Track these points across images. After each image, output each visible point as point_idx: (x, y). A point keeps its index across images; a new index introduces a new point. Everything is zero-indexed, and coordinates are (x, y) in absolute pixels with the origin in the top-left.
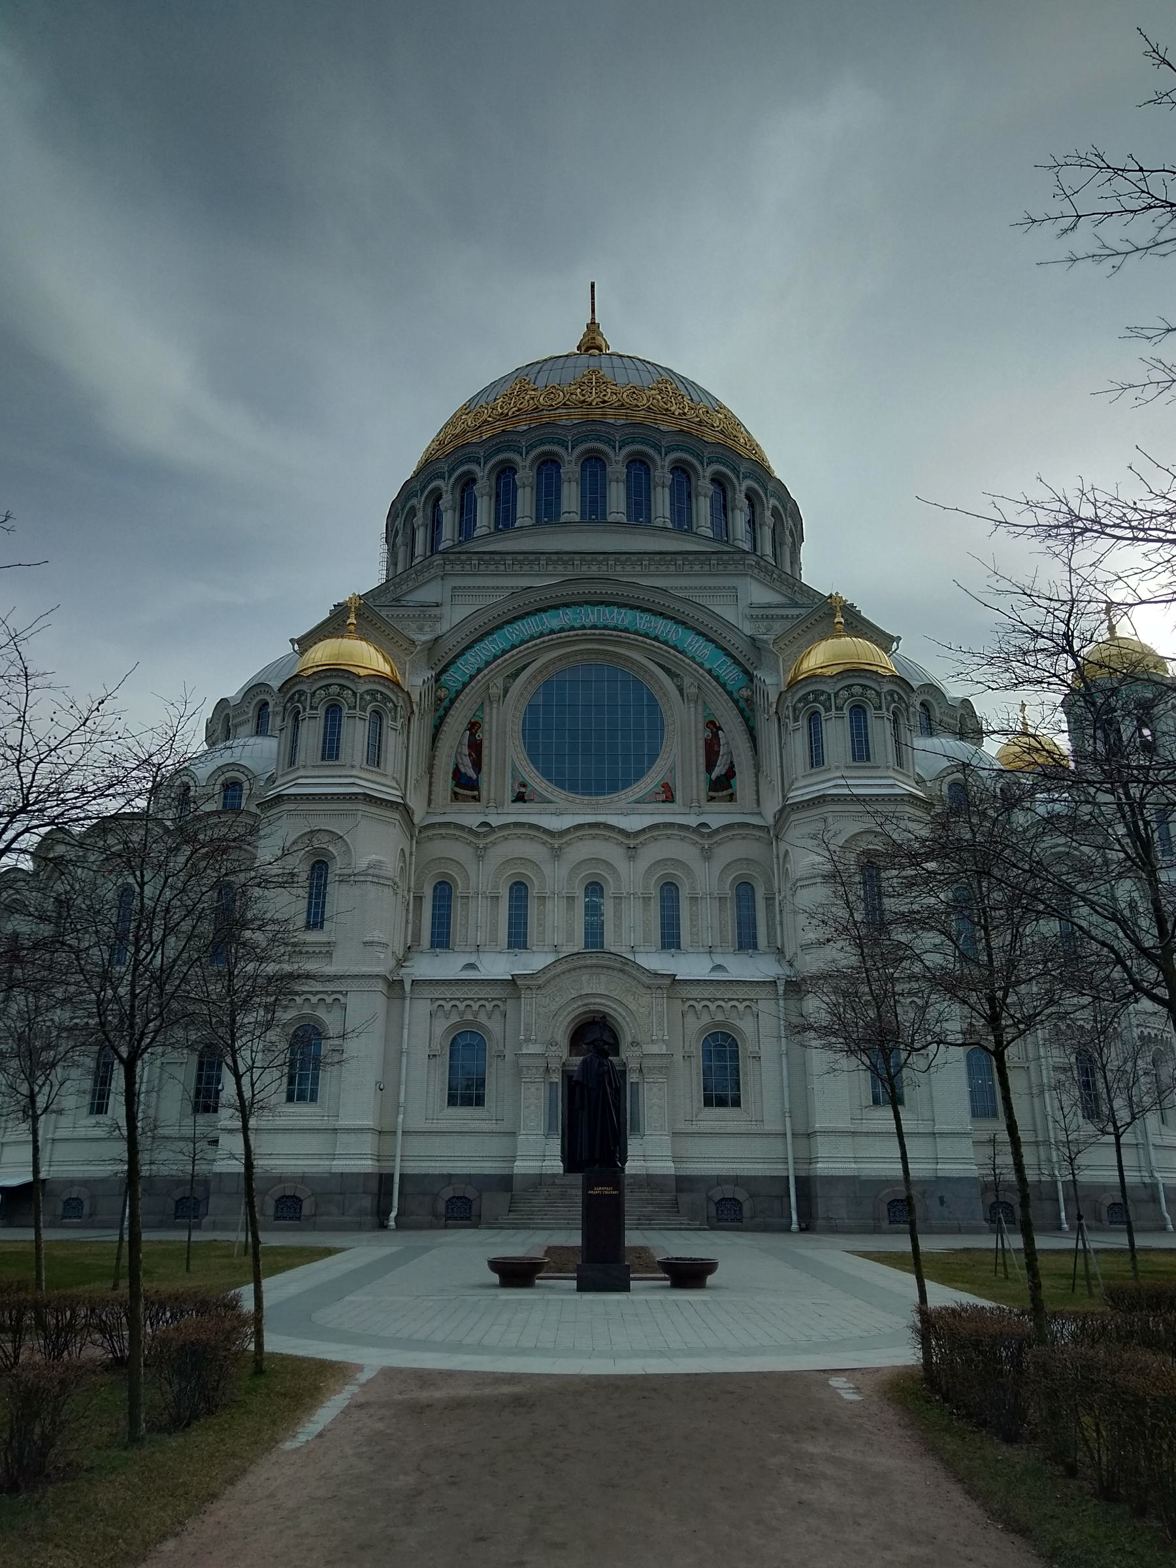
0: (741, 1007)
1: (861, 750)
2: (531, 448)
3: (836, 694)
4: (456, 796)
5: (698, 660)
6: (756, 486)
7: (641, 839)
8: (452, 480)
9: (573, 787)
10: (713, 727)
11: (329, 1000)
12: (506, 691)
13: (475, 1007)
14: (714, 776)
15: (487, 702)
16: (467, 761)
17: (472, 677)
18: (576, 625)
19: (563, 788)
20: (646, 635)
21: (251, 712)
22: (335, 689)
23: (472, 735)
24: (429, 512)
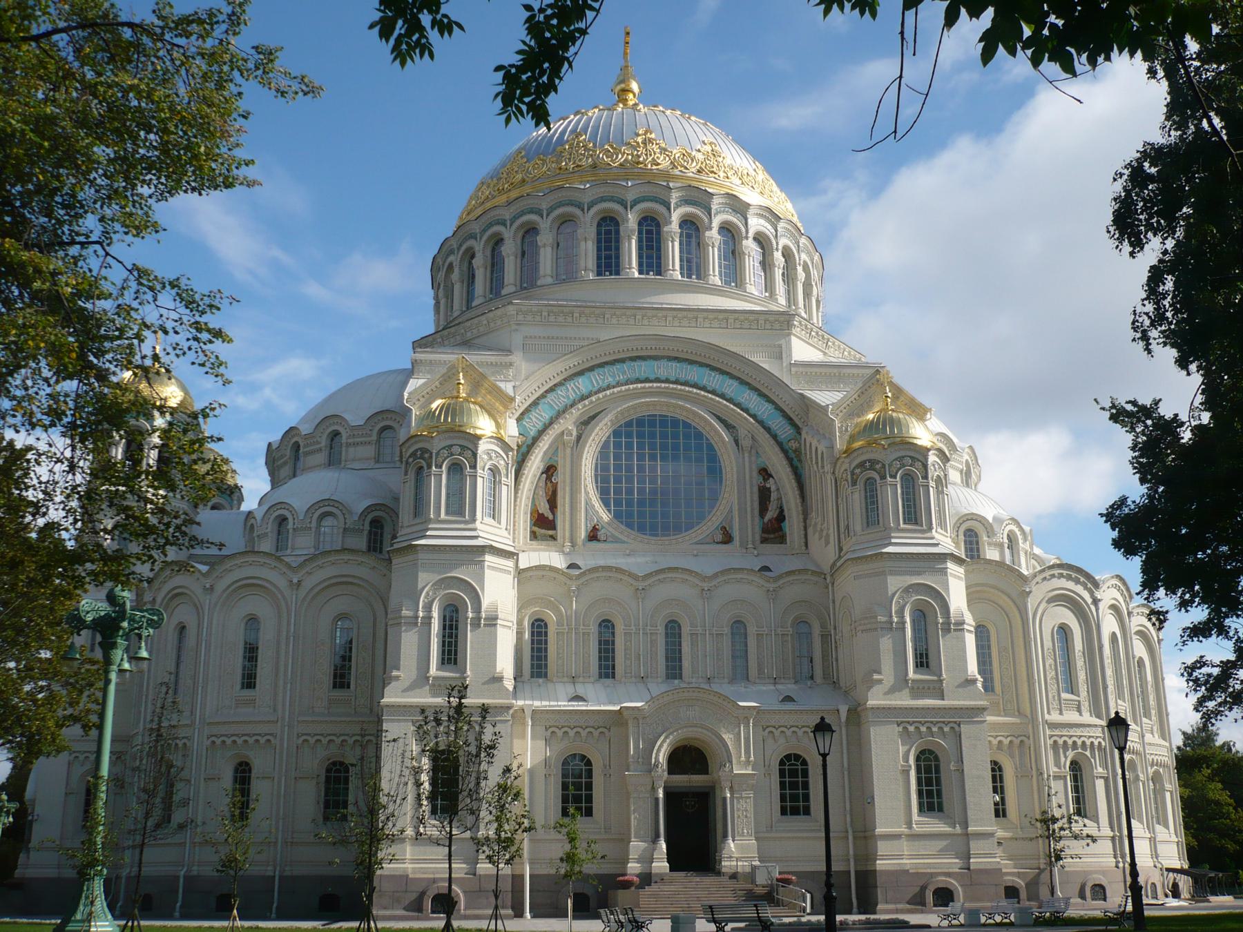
4: (534, 536)
9: (642, 529)
10: (765, 473)
14: (766, 519)
21: (324, 441)
23: (549, 478)
24: (488, 253)
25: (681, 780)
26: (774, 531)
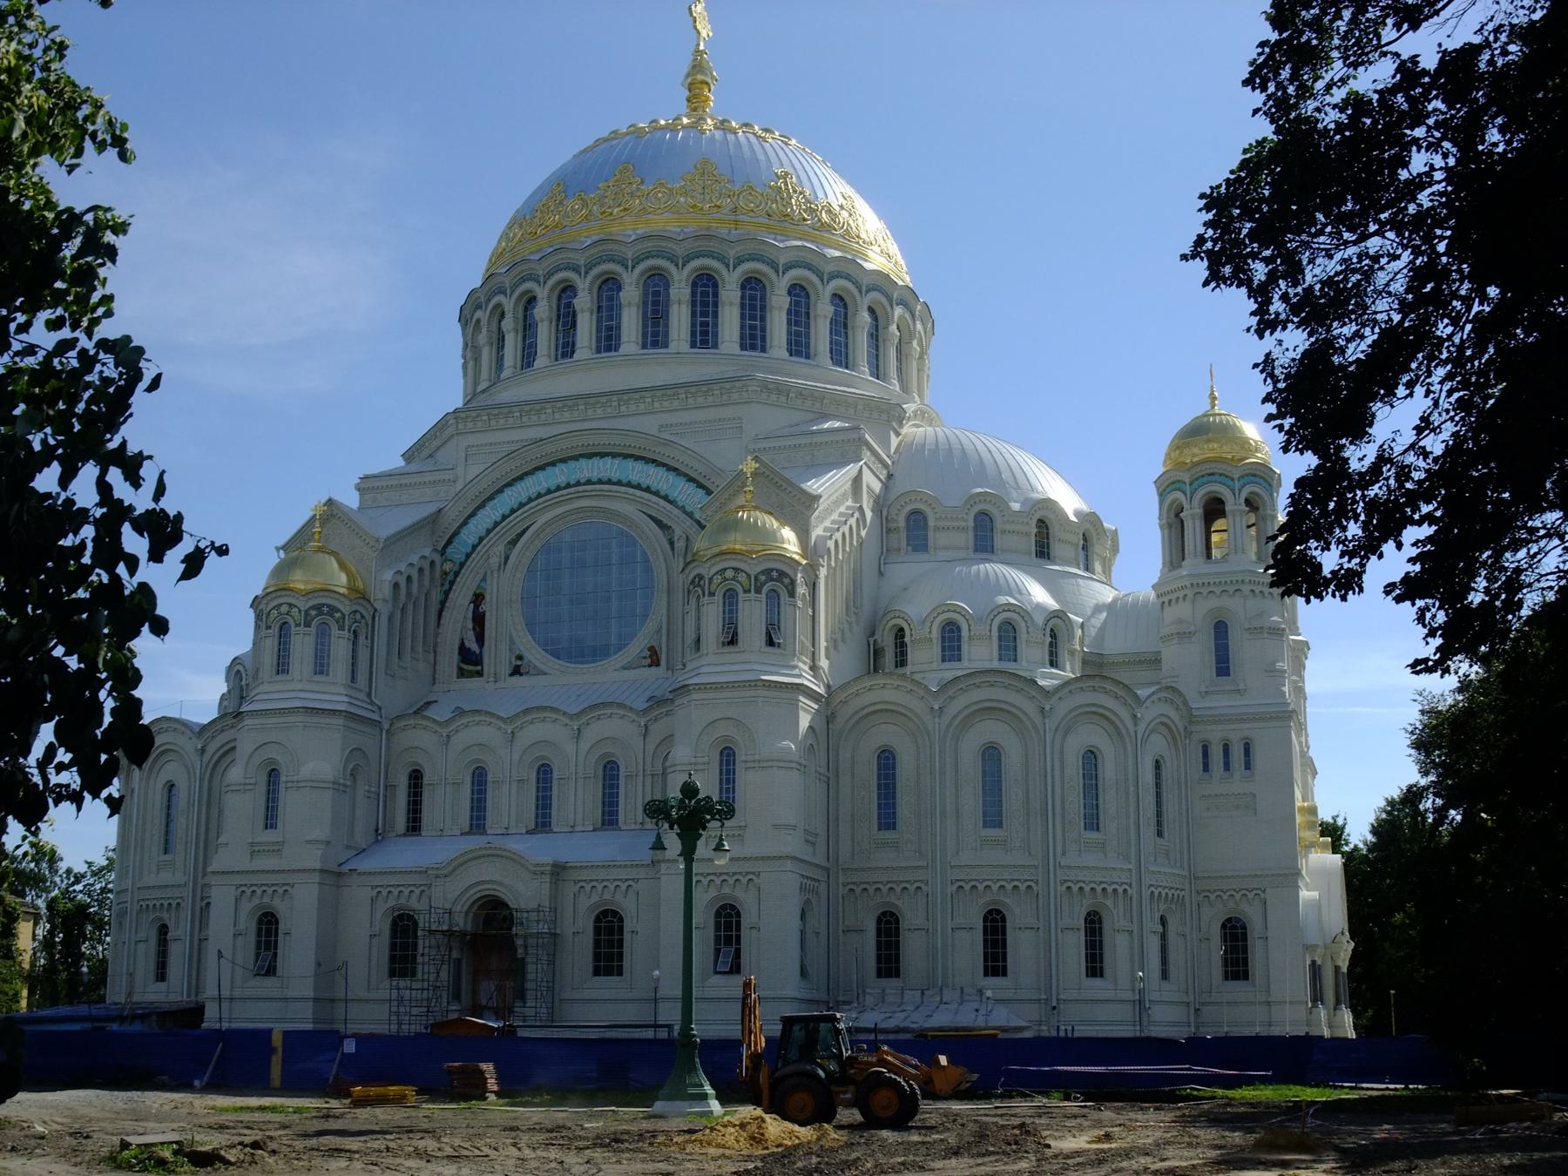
2: (550, 274)
3: (711, 580)
12: (507, 558)
16: (471, 635)
17: (474, 547)
20: (638, 487)
22: (284, 609)
23: (476, 607)
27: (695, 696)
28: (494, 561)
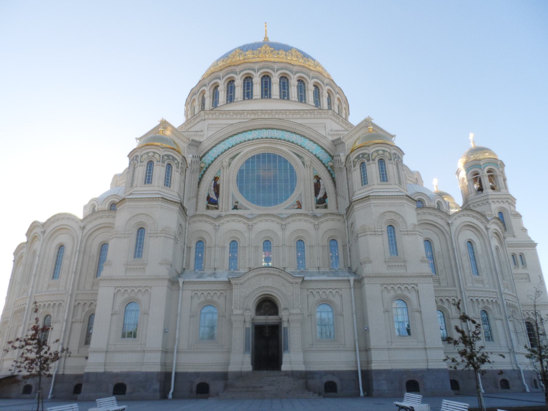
0: (334, 292)
1: (383, 177)
2: (241, 71)
3: (372, 154)
4: (208, 208)
5: (310, 150)
6: (331, 89)
7: (288, 221)
8: (209, 87)
10: (318, 178)
11: (143, 290)
12: (230, 164)
13: (212, 294)
14: (318, 198)
15: (222, 169)
17: (215, 159)
18: (259, 137)
19: (254, 203)
22: (151, 154)
23: (215, 182)
25: (262, 319)
26: (322, 202)
27: (372, 201)
28: (225, 164)
